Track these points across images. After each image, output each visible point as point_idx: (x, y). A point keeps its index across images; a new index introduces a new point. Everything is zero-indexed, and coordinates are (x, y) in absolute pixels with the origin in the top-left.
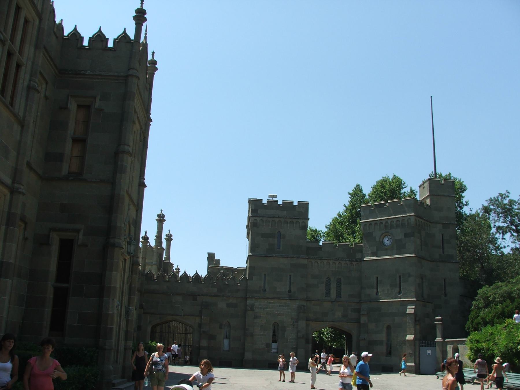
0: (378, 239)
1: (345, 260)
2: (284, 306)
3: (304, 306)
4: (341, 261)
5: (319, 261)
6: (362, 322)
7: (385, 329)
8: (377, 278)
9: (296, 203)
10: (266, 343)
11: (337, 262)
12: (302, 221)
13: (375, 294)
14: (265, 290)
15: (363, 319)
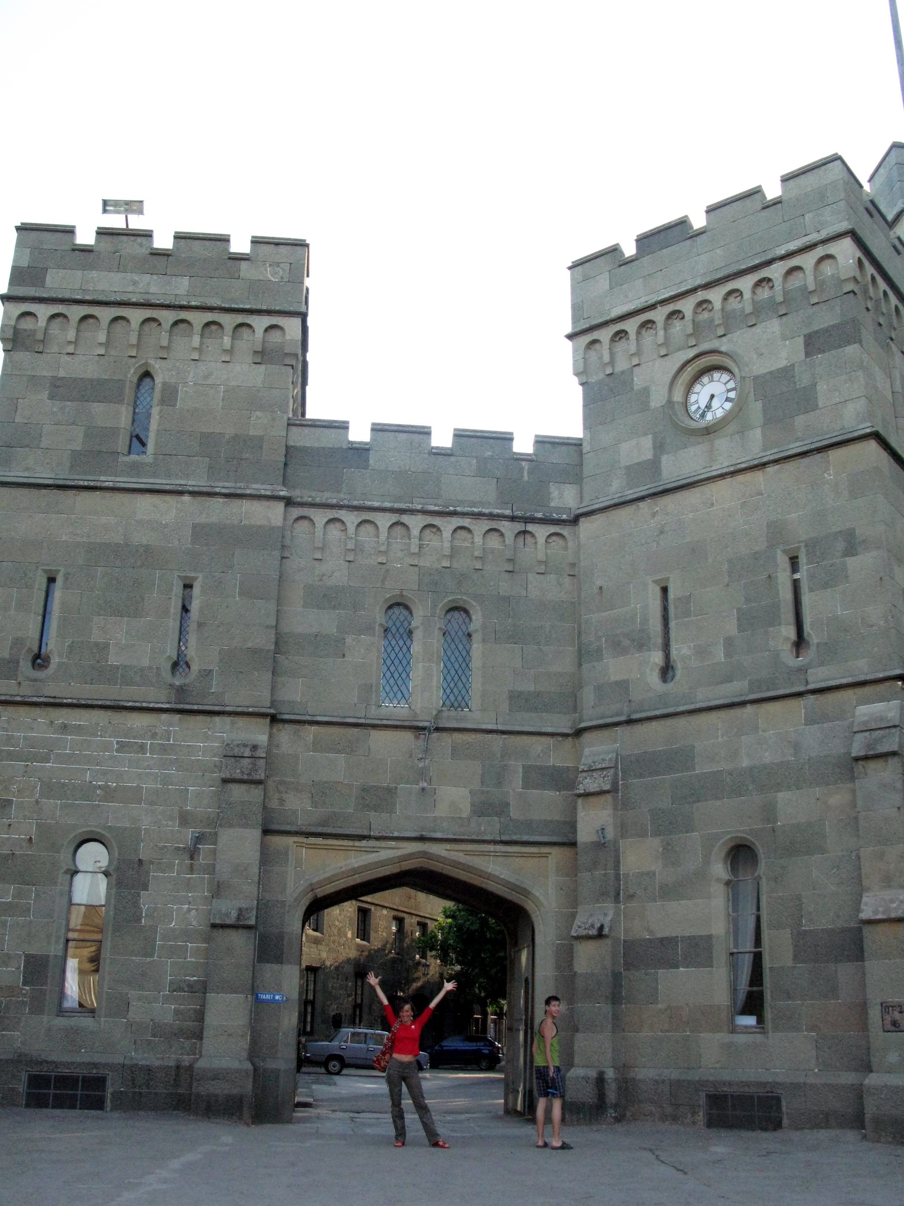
0: (657, 399)
1: (492, 516)
2: (142, 748)
3: (255, 747)
4: (466, 522)
5: (351, 519)
6: (585, 835)
7: (719, 869)
8: (665, 590)
9: (240, 245)
10: (29, 959)
11: (448, 525)
12: (267, 321)
13: (654, 678)
14: (39, 660)
15: (592, 821)
